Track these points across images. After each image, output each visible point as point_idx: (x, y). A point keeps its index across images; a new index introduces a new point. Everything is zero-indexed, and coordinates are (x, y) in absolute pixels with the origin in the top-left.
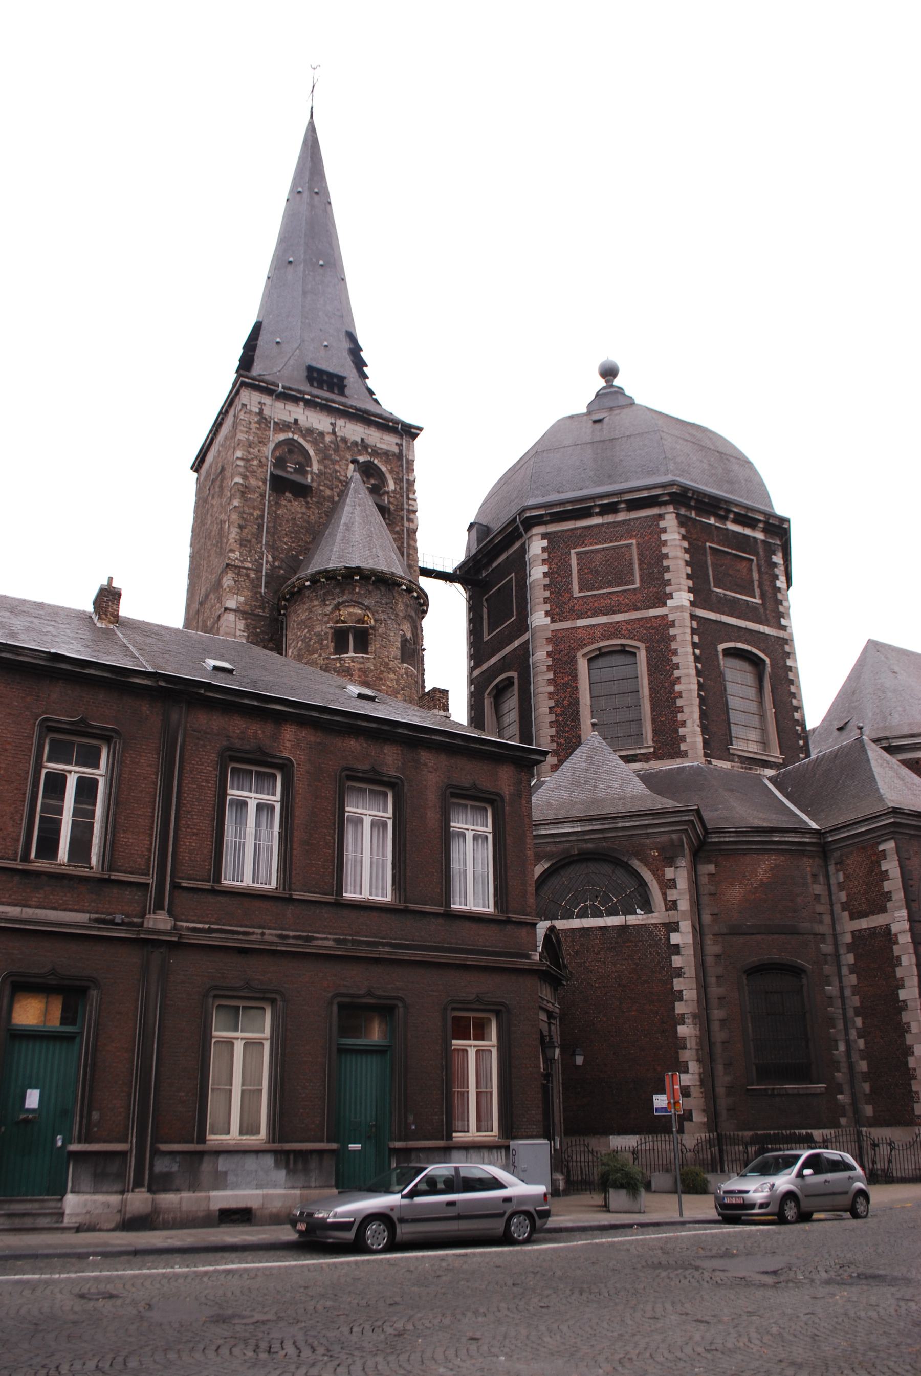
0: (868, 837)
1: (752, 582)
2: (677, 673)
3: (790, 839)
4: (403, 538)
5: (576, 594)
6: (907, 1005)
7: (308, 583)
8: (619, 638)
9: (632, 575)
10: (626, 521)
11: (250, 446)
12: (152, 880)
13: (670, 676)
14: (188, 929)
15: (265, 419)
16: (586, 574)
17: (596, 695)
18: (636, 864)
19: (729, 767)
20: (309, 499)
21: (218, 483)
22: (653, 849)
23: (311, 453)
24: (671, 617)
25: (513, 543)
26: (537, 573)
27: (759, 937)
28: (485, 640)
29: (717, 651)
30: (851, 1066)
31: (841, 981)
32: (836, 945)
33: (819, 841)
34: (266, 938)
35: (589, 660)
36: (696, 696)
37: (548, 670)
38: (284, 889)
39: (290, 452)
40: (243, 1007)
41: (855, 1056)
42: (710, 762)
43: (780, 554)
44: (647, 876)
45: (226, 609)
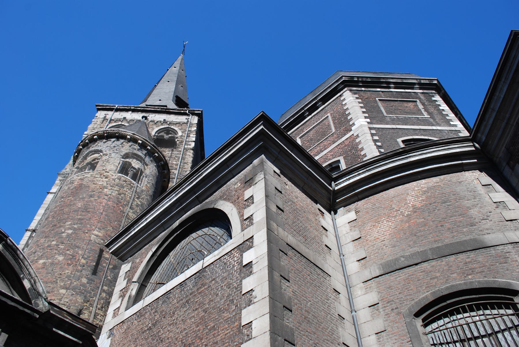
27: (425, 265)
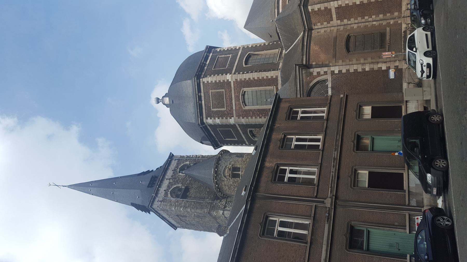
0: (307, 15)
1: (225, 57)
2: (252, 79)
3: (306, 39)
4: (204, 159)
5: (225, 109)
6: (362, 1)
7: (217, 186)
8: (239, 96)
9: (220, 92)
10: (204, 93)
11: (171, 205)
12: (314, 204)
13: (252, 81)
14: (331, 194)
15: (163, 200)
16: (219, 106)
17: (257, 104)
18: (312, 84)
19: (282, 63)
20: (190, 187)
21: (181, 218)
22: (307, 79)
23: (175, 186)
24: (234, 80)
25: (208, 129)
26: (218, 121)
27: (337, 49)
28: (237, 140)
29: (245, 67)
30: (381, 20)
31: (353, 24)
32: (341, 26)
33: (307, 31)
34: (334, 171)
35: (246, 106)
36: (259, 73)
37: (248, 118)
38: (318, 166)
39: (174, 193)
40: (357, 179)
41: (378, 19)
42: (280, 69)
43: (217, 49)
44: (315, 81)
45: (223, 214)
